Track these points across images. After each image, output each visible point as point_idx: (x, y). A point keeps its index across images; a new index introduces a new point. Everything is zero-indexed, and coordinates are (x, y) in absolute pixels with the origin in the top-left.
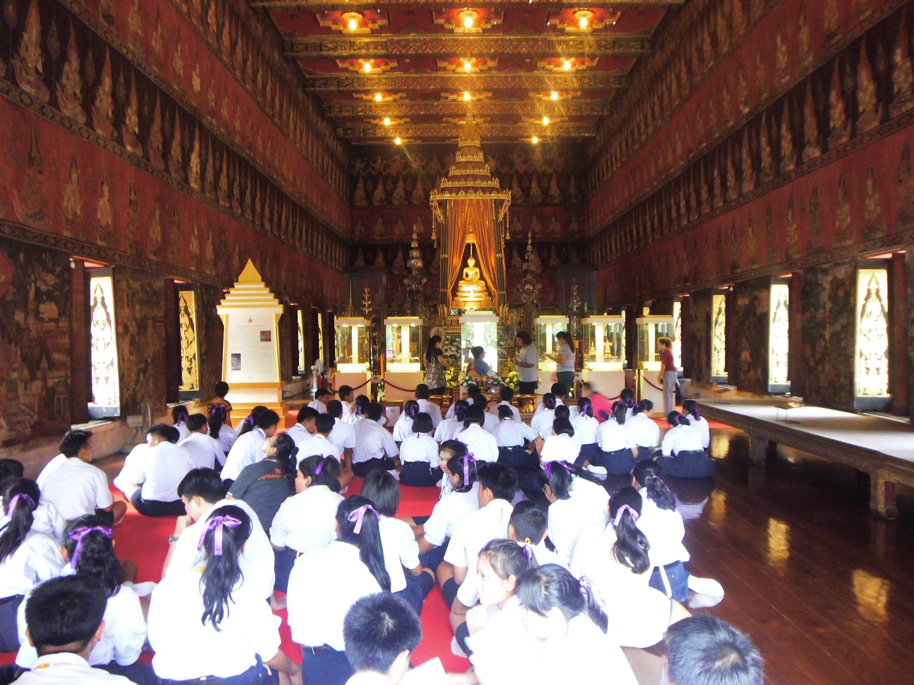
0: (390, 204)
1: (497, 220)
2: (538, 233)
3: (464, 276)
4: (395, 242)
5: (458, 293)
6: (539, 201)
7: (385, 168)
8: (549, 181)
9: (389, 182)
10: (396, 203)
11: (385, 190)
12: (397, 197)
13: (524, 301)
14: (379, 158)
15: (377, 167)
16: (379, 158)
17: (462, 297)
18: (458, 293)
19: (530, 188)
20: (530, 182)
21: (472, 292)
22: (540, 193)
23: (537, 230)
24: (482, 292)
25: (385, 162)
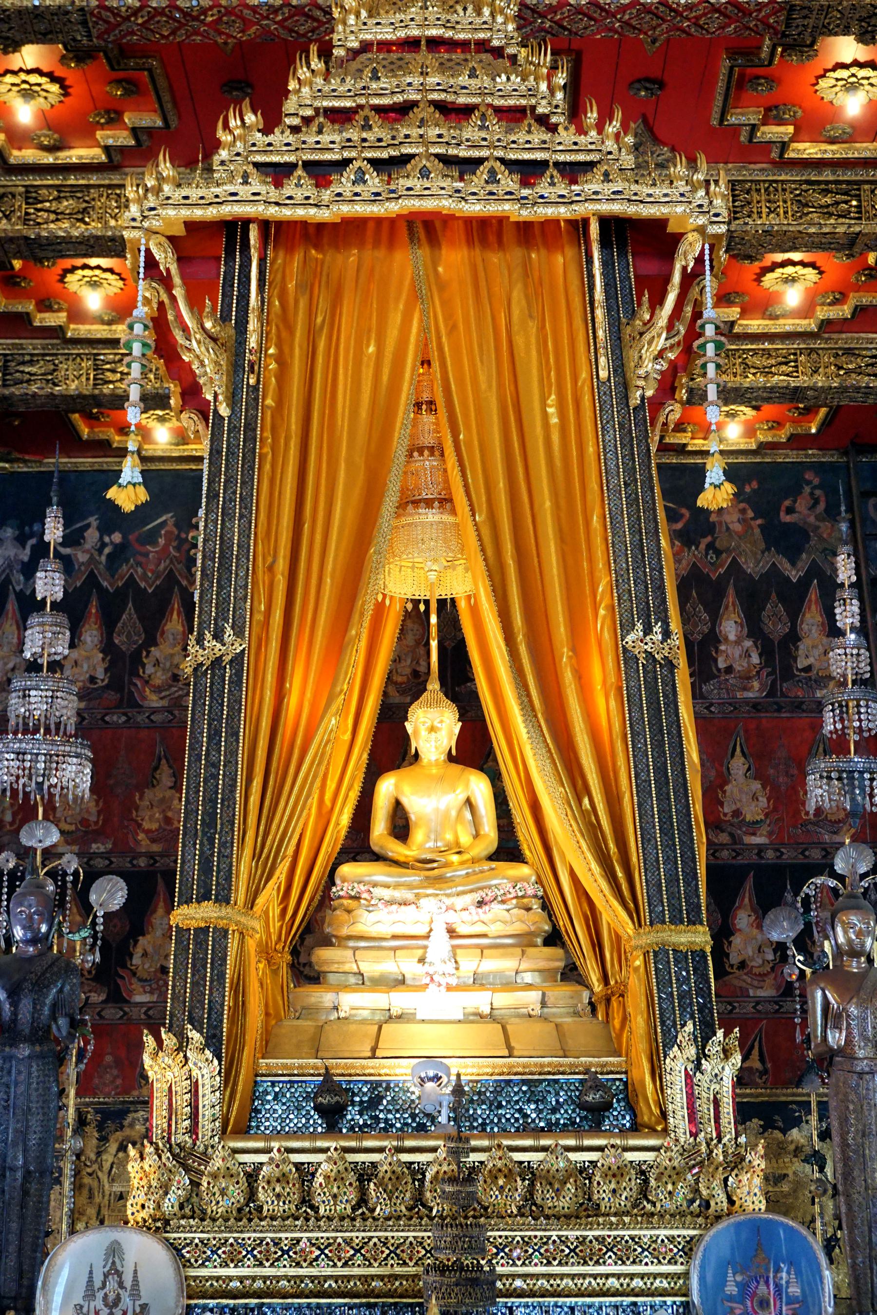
0: (132, 703)
1: (625, 387)
2: (753, 827)
3: (379, 827)
4: (142, 862)
5: (324, 955)
6: (755, 690)
7: (119, 554)
8: (795, 612)
9: (129, 615)
10: (153, 700)
11: (108, 648)
12: (159, 678)
13: (836, 1038)
14: (93, 521)
15: (82, 557)
16: (93, 521)
17: (363, 982)
18: (324, 955)
19: (713, 639)
20: (715, 617)
21: (439, 944)
22: (755, 659)
23: (753, 811)
24: (524, 941)
25: (117, 537)
